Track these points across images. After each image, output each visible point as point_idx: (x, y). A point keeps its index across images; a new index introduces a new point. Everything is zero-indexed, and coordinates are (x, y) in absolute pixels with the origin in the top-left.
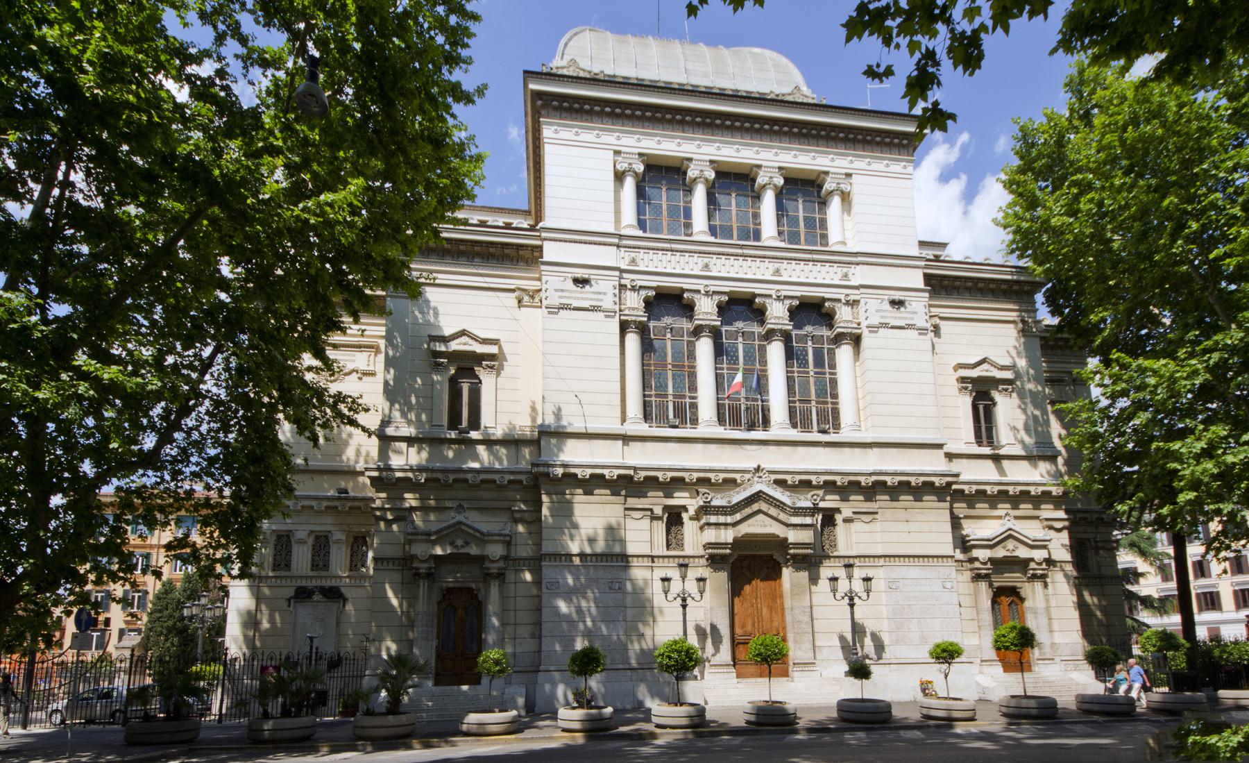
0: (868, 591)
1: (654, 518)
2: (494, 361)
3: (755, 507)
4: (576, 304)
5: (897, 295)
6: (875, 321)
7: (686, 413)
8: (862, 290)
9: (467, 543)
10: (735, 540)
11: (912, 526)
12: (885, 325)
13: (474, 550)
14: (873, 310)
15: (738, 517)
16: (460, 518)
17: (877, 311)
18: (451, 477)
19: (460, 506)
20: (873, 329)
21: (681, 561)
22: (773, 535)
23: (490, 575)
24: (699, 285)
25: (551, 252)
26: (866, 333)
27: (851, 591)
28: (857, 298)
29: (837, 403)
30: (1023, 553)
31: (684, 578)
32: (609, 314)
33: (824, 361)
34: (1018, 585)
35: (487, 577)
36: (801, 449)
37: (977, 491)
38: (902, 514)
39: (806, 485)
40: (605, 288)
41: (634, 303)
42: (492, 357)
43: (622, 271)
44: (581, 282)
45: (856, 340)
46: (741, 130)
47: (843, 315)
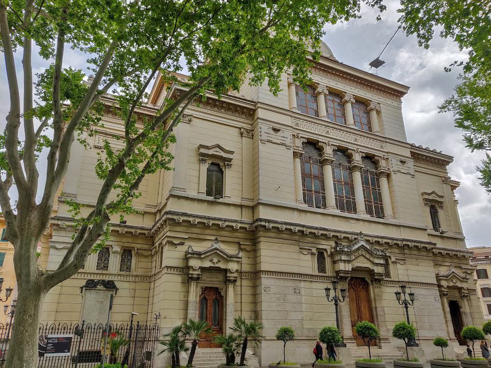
0: (412, 301)
1: (313, 254)
3: (360, 252)
4: (274, 141)
6: (395, 168)
7: (322, 202)
9: (219, 261)
12: (399, 171)
13: (222, 265)
16: (216, 246)
18: (212, 222)
19: (216, 239)
20: (395, 172)
23: (229, 281)
24: (326, 140)
25: (261, 113)
31: (335, 289)
33: (376, 184)
35: (227, 281)
40: (287, 134)
44: (276, 130)
45: (388, 176)
46: (335, 75)
47: (383, 163)
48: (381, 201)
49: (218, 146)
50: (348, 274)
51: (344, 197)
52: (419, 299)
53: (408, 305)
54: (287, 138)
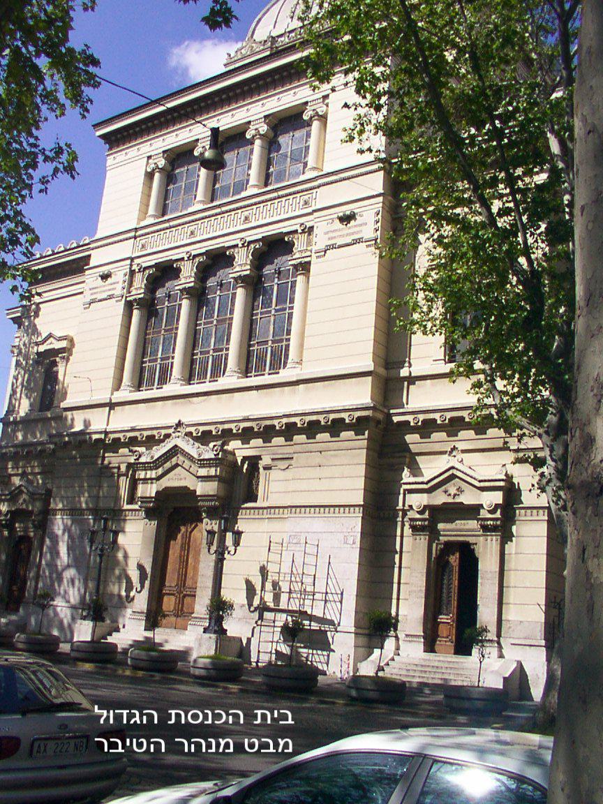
2: (66, 352)
3: (174, 460)
5: (347, 210)
8: (316, 214)
10: (157, 493)
12: (333, 247)
15: (160, 471)
17: (326, 233)
22: (186, 487)
26: (314, 260)
30: (468, 498)
34: (471, 540)
36: (236, 395)
38: (316, 458)
39: (227, 435)
41: (140, 283)
42: (63, 350)
43: (132, 259)
45: (305, 267)
47: (300, 243)
50: (150, 502)
51: (211, 352)
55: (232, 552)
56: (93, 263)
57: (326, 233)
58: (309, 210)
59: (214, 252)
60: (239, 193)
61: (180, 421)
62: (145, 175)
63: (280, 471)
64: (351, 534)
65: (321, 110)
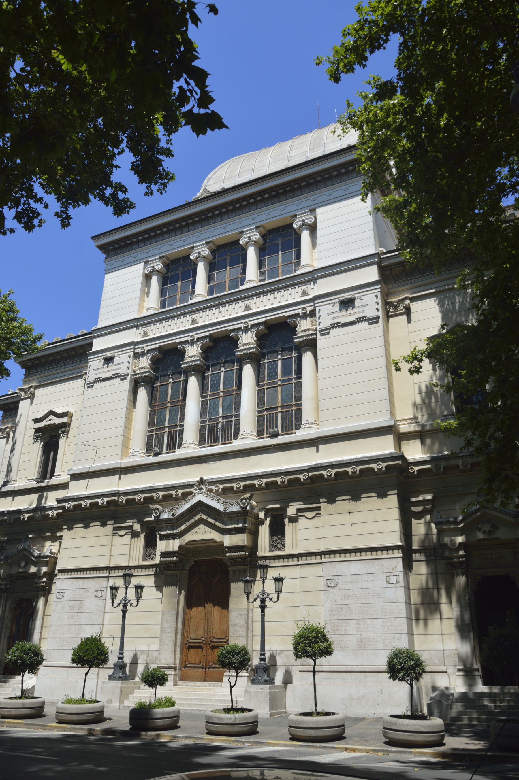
0: (279, 592)
4: (104, 376)
6: (326, 323)
10: (180, 547)
11: (355, 518)
14: (328, 312)
17: (328, 314)
20: (325, 332)
21: (127, 572)
22: (212, 539)
27: (263, 593)
28: (312, 308)
29: (300, 405)
32: (123, 377)
37: (289, 481)
41: (145, 362)
45: (311, 345)
48: (299, 398)
49: (52, 413)
52: (340, 585)
53: (268, 600)
54: (123, 363)
55: (275, 599)
56: (94, 349)
57: (328, 314)
58: (311, 297)
59: (216, 337)
60: (237, 286)
61: (201, 479)
62: (143, 277)
63: (308, 520)
64: (393, 574)
65: (310, 220)
